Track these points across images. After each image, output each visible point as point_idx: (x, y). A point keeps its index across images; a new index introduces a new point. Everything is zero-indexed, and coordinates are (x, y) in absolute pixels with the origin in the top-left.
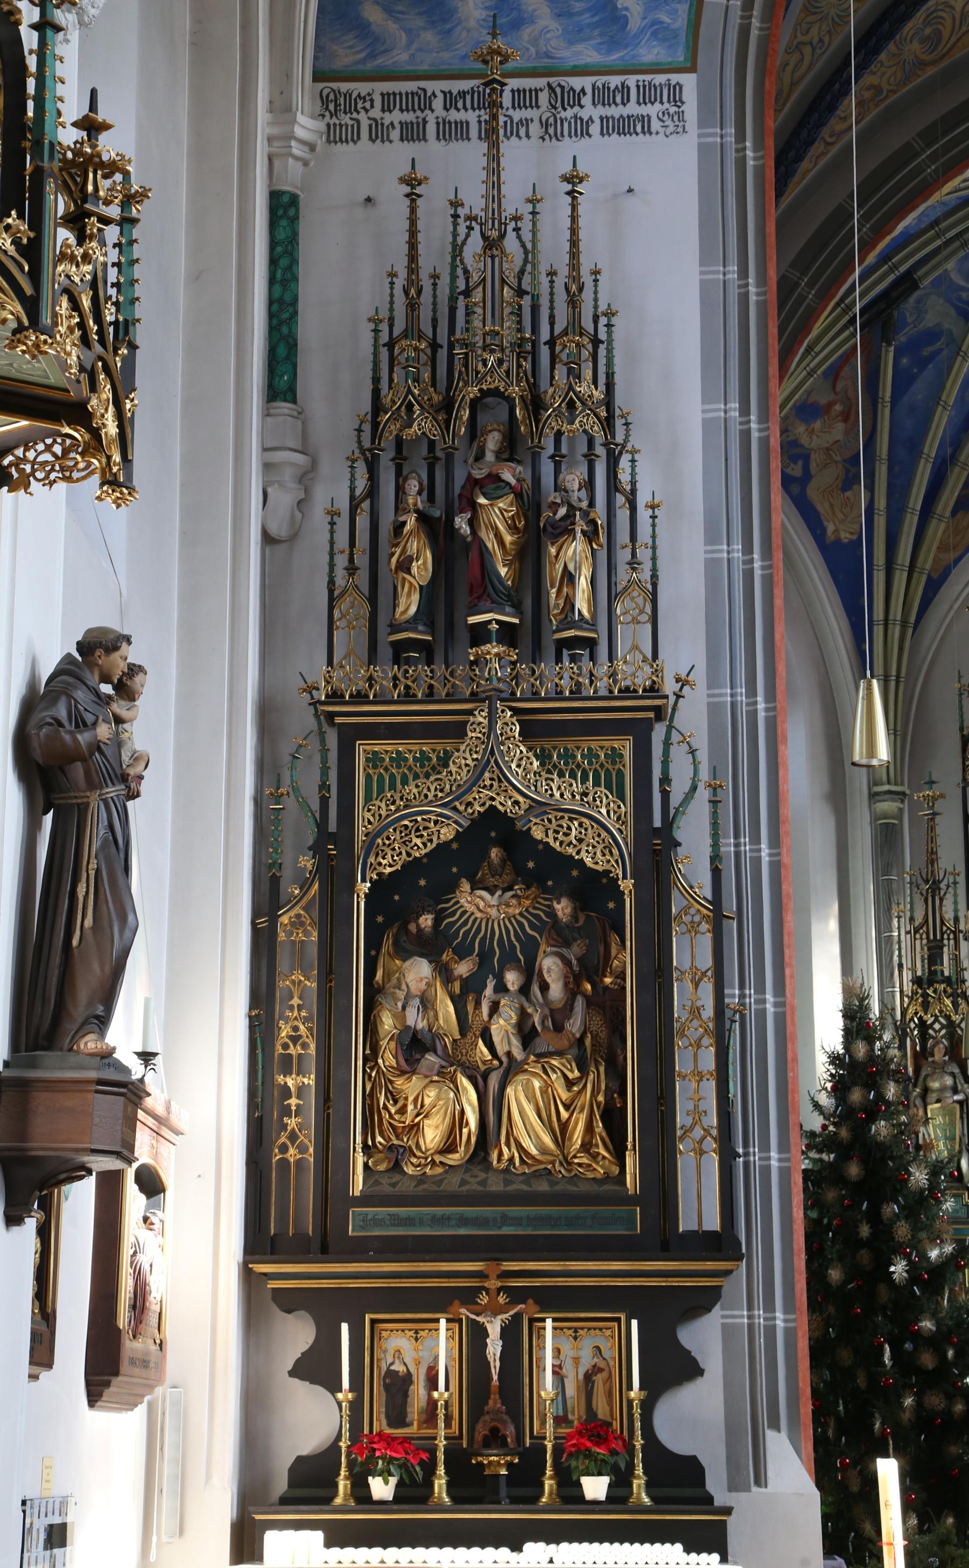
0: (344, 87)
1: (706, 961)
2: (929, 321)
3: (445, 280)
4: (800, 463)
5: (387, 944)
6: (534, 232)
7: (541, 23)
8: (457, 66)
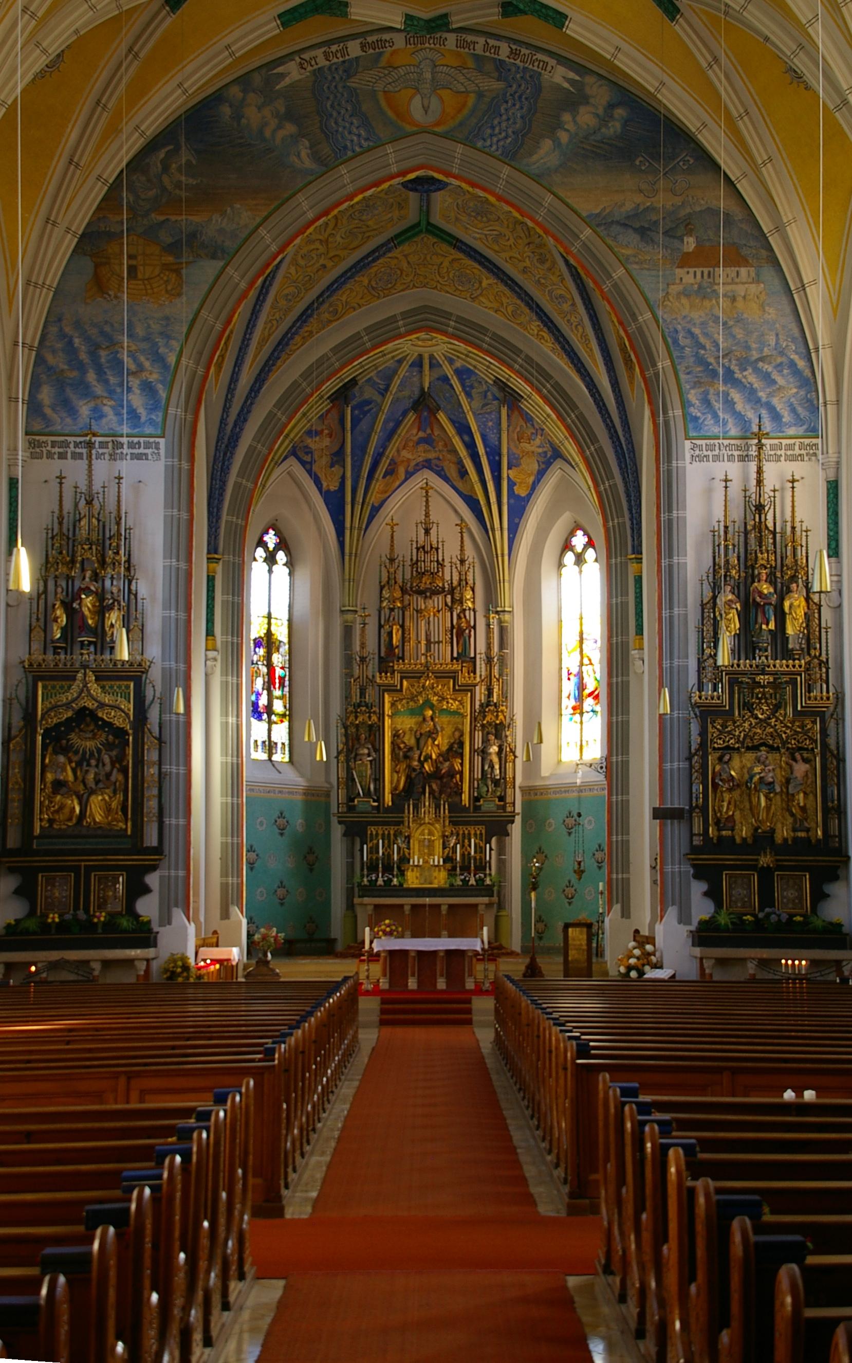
0: (37, 438)
2: (366, 396)
3: (72, 515)
5: (50, 749)
6: (104, 498)
7: (110, 417)
8: (79, 432)
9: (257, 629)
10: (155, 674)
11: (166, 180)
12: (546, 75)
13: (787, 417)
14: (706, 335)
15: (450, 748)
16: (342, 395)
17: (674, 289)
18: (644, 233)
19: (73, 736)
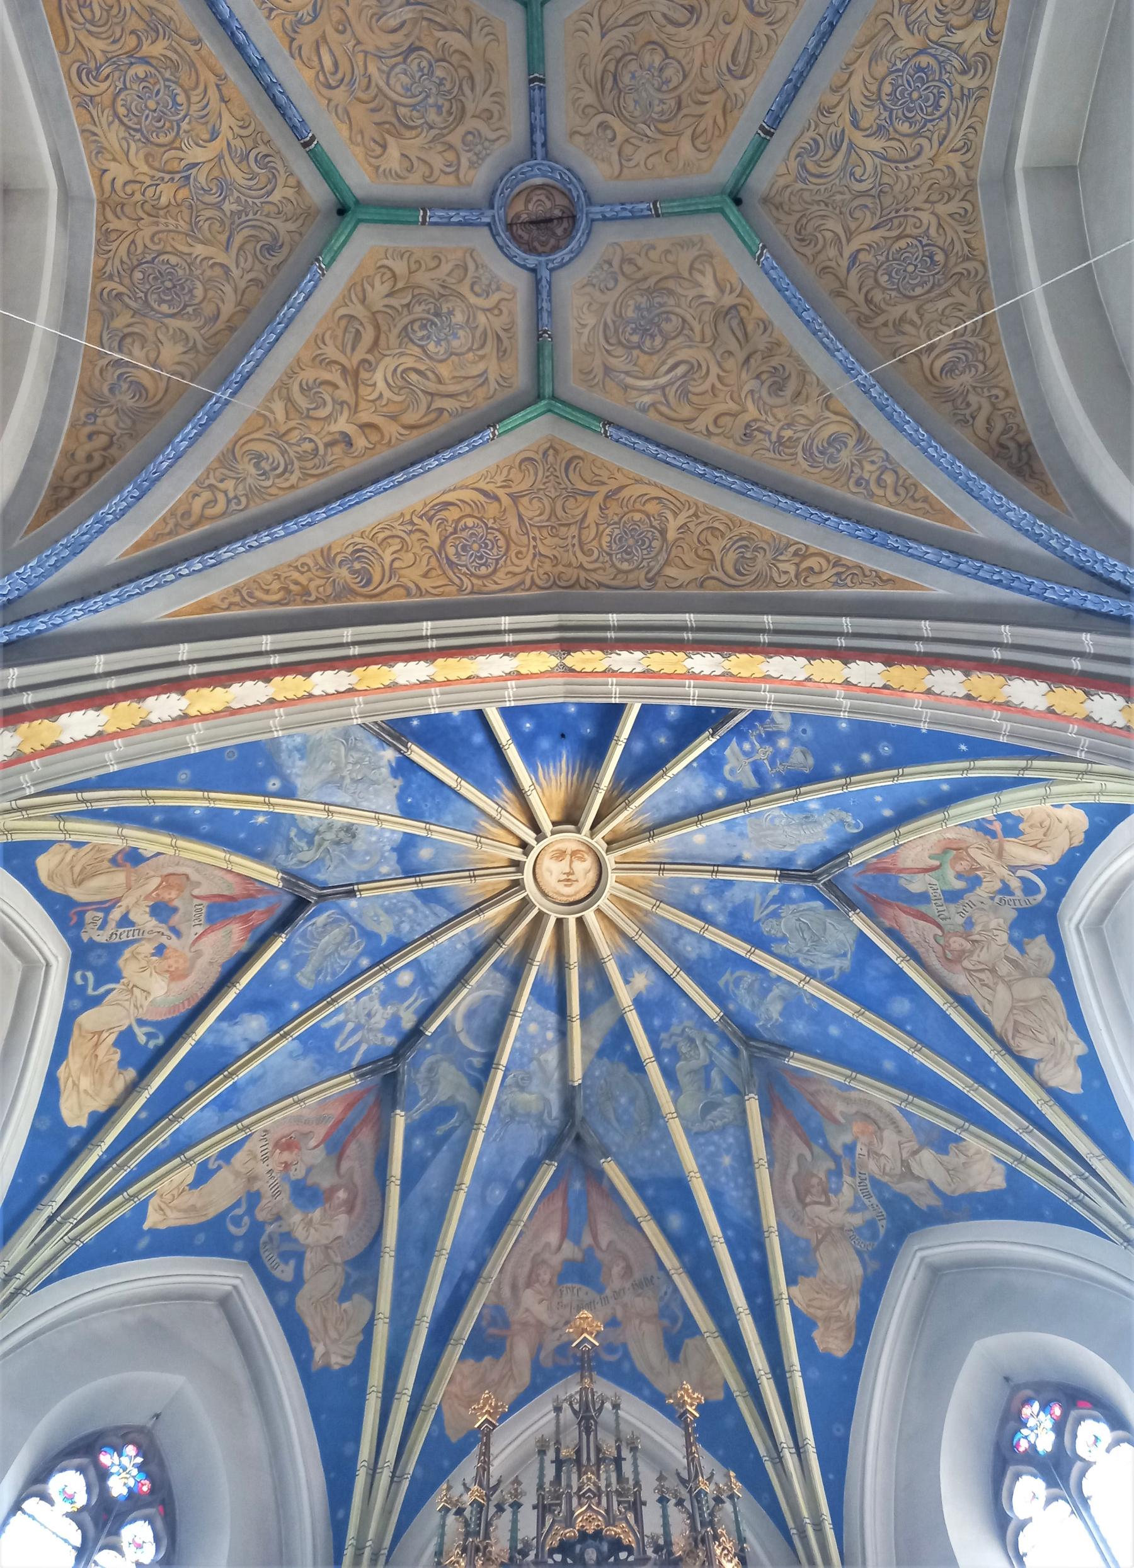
2: (443, 1093)
4: (292, 1263)
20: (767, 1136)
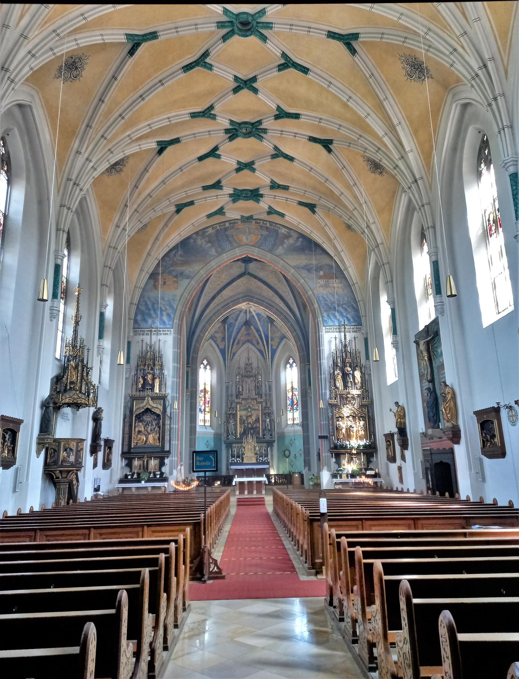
1: (169, 423)
9: (201, 387)
10: (169, 398)
11: (175, 259)
12: (280, 230)
13: (352, 320)
14: (328, 297)
15: (256, 420)
16: (224, 321)
17: (318, 285)
18: (309, 270)
19: (144, 417)
20: (271, 327)
